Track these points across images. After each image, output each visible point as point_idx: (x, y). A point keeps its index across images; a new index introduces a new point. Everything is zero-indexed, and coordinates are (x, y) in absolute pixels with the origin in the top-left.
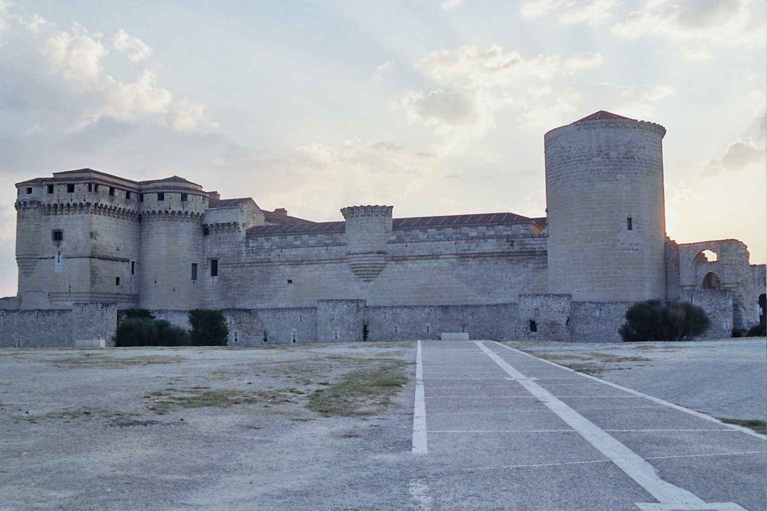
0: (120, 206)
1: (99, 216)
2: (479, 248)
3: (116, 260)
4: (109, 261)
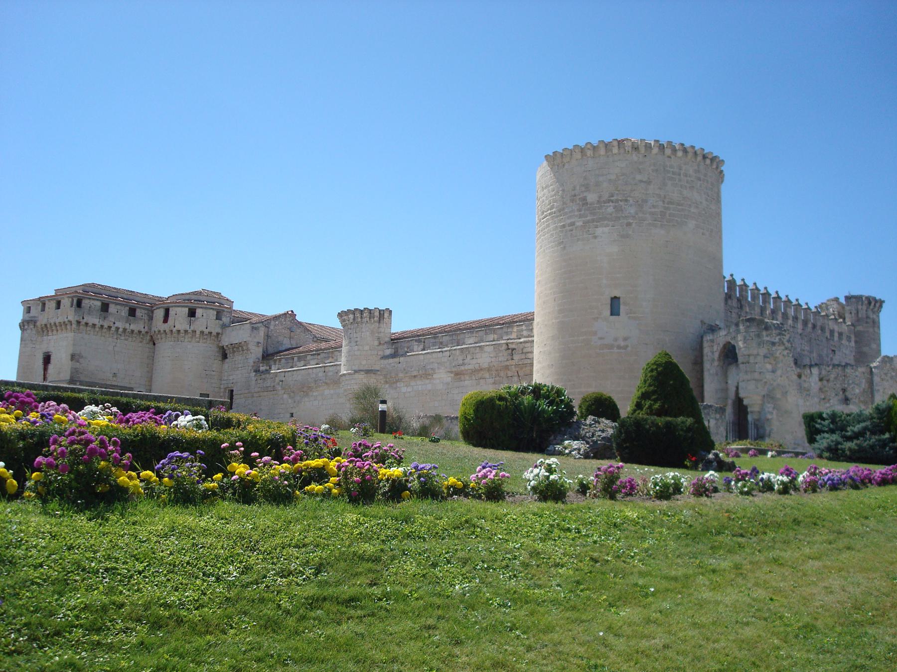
0: (118, 324)
2: (474, 361)
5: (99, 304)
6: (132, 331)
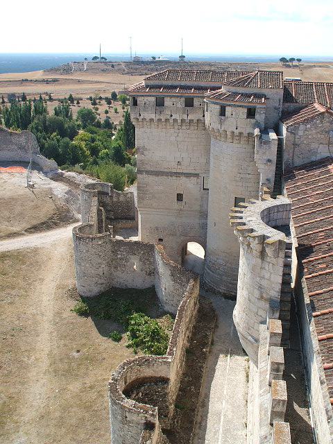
1: (148, 130)
3: (178, 174)
5: (153, 99)
6: (191, 121)
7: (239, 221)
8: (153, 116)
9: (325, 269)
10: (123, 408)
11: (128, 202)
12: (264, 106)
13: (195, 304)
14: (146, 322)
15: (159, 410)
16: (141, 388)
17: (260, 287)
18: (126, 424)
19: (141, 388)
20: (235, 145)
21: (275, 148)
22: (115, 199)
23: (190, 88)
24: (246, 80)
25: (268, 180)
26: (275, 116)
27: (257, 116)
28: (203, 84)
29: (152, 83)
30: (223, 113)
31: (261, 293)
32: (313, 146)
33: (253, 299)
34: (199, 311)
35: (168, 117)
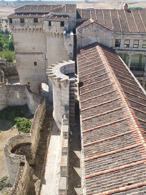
1: (18, 34)
3: (34, 53)
4: (28, 55)
5: (19, 19)
7: (50, 72)
8: (20, 27)
9: (88, 90)
10: (10, 157)
11: (14, 67)
12: (68, 21)
13: (44, 110)
14: (23, 120)
15: (26, 156)
16: (19, 148)
17: (61, 101)
18: (12, 164)
19: (19, 148)
20: (57, 39)
21: (72, 39)
22: (8, 66)
23: (35, 14)
24: (60, 9)
25: (70, 54)
26: (73, 25)
27: (65, 25)
28: (42, 11)
29: (18, 12)
30: (50, 25)
31: (61, 103)
32: (90, 37)
33: (59, 106)
34: (46, 113)
35: (27, 28)
